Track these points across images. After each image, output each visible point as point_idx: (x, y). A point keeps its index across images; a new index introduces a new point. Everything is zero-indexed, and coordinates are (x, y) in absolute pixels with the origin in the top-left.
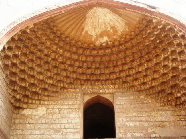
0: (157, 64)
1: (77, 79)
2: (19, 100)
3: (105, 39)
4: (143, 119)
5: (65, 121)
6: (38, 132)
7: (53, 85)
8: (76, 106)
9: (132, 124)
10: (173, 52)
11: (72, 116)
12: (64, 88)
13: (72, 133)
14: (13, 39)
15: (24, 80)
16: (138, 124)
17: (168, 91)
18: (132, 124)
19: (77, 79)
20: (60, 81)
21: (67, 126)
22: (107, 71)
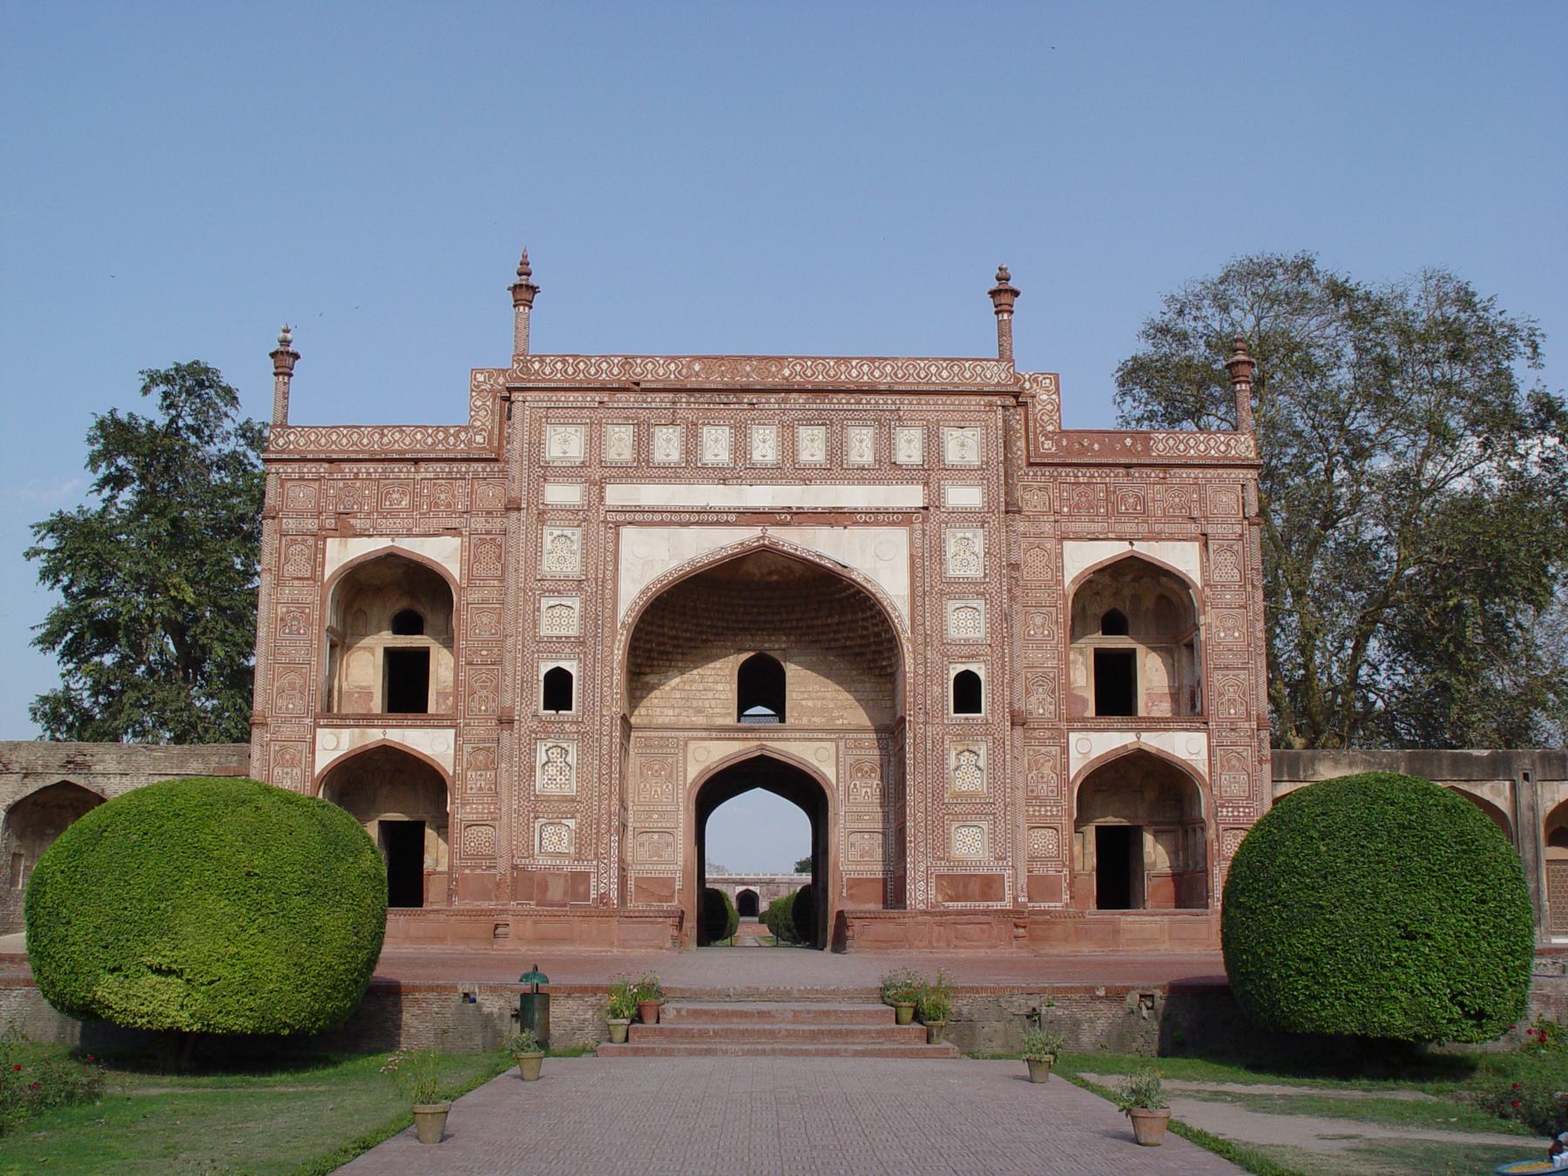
0: (852, 621)
1: (727, 628)
2: (639, 666)
3: (775, 578)
4: (828, 695)
5: (710, 695)
6: (671, 712)
7: (690, 640)
8: (727, 672)
9: (810, 703)
10: (873, 617)
11: (720, 687)
12: (706, 641)
13: (721, 715)
14: (646, 612)
15: (650, 641)
16: (819, 704)
17: (869, 657)
18: (810, 703)
19: (727, 628)
20: (701, 633)
21: (713, 703)
22: (777, 617)
